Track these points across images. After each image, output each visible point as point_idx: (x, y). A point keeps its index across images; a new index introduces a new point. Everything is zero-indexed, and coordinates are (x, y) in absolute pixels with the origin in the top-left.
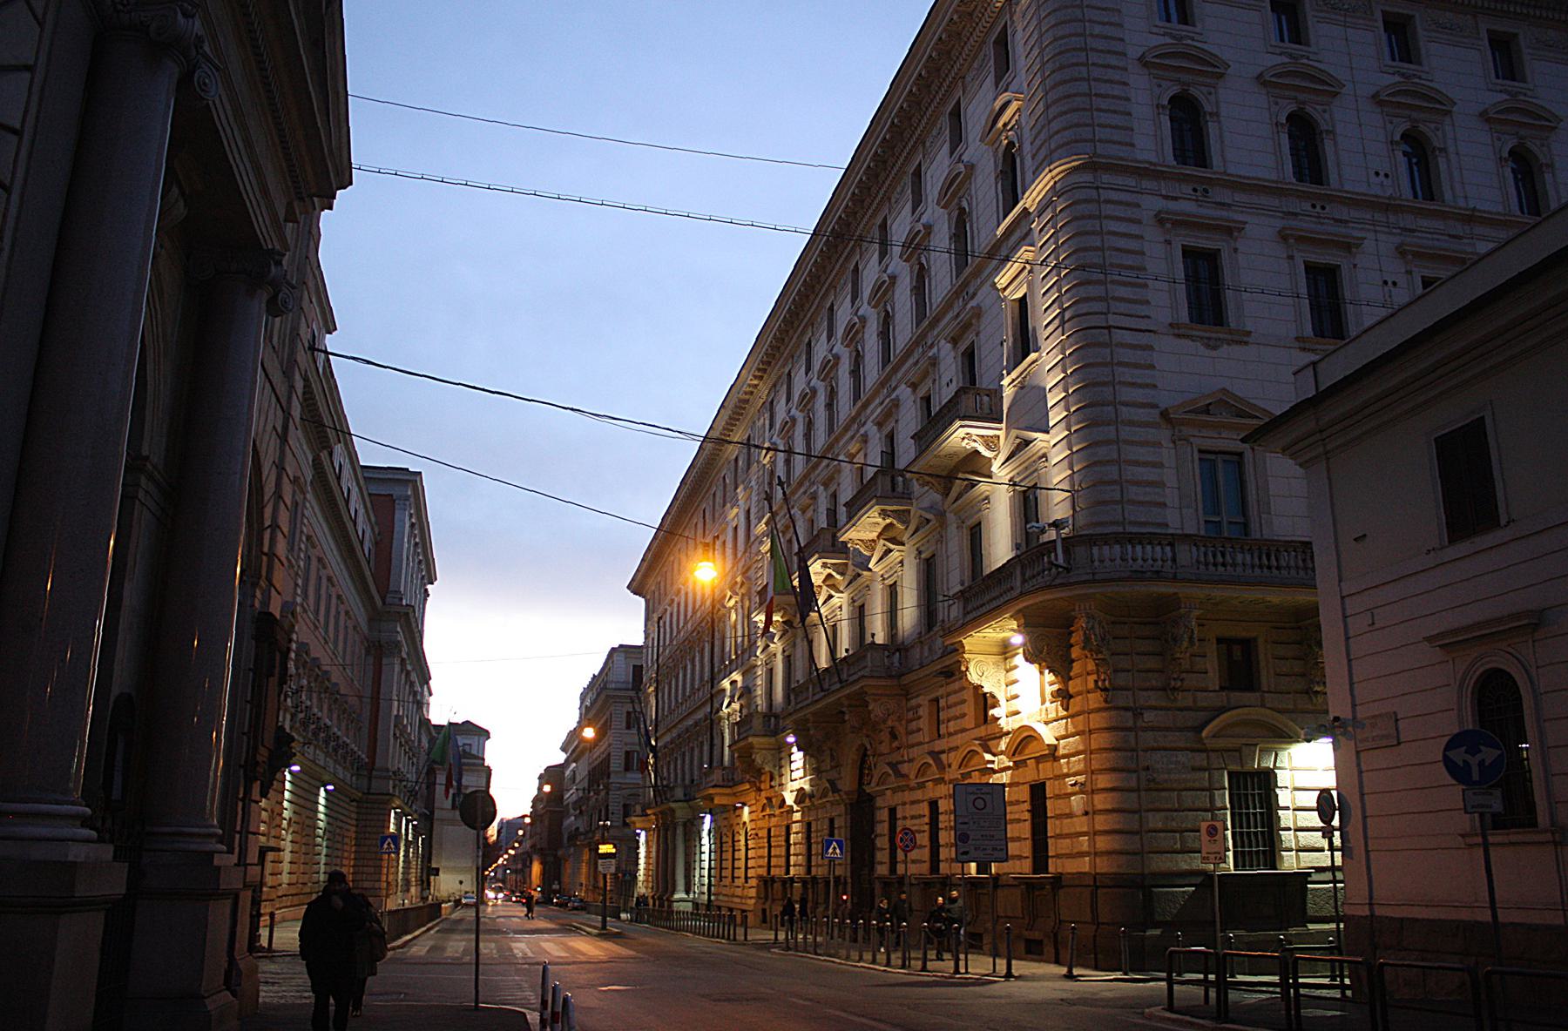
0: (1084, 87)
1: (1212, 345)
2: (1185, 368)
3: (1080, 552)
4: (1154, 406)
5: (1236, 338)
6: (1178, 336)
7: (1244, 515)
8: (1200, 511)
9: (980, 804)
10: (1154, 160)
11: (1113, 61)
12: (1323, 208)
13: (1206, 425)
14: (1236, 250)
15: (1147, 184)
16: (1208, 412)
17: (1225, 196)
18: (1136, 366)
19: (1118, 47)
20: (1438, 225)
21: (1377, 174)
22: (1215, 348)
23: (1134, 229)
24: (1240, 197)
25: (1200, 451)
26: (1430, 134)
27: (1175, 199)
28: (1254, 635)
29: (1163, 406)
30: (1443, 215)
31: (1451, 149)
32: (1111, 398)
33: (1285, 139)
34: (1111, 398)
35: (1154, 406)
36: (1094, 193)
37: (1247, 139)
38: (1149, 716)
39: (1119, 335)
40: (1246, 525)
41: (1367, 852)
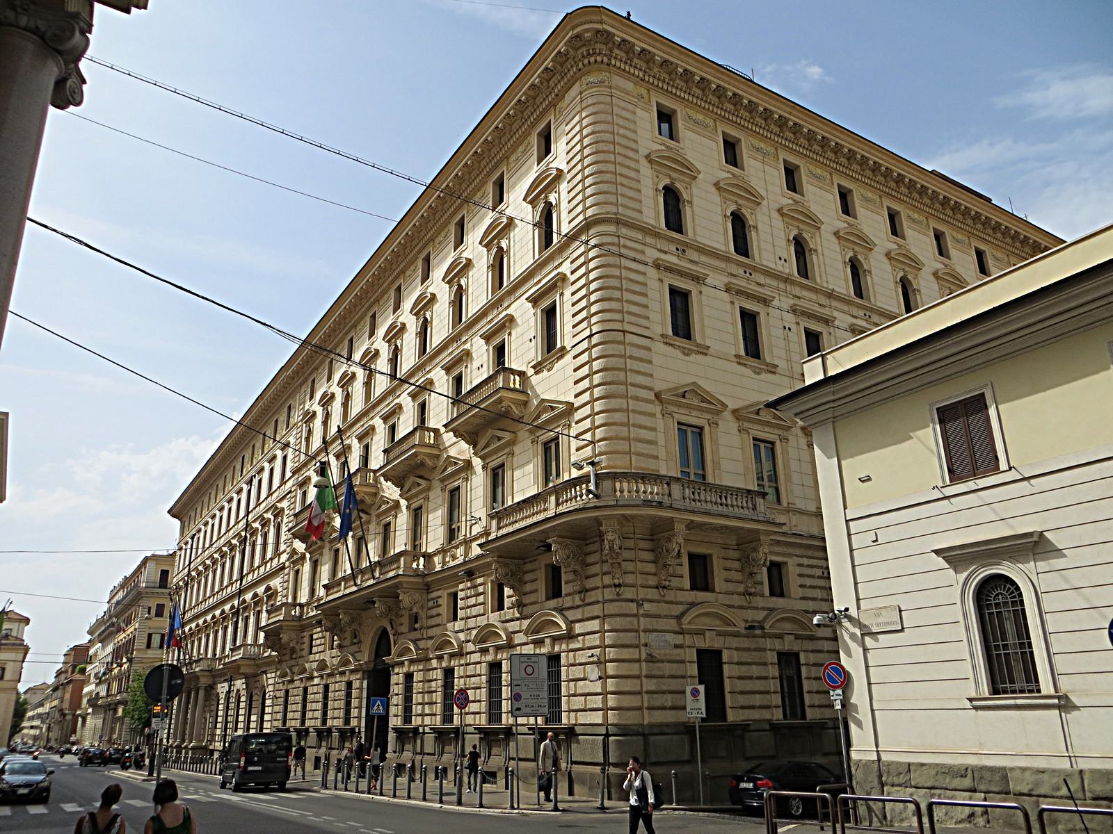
0: (611, 167)
1: (686, 353)
2: (671, 367)
3: (607, 484)
4: (651, 389)
5: (700, 350)
6: (666, 343)
7: (703, 469)
8: (679, 466)
9: (529, 670)
10: (654, 224)
11: (631, 154)
12: (751, 274)
13: (680, 405)
14: (701, 292)
15: (649, 240)
16: (684, 396)
17: (694, 256)
18: (641, 360)
19: (633, 145)
20: (813, 296)
21: (780, 259)
22: (687, 355)
23: (641, 268)
24: (703, 259)
25: (679, 423)
26: (808, 239)
27: (665, 252)
28: (710, 552)
29: (657, 389)
30: (815, 291)
31: (820, 251)
32: (624, 380)
33: (730, 225)
34: (624, 380)
35: (651, 389)
36: (615, 240)
37: (708, 222)
38: (647, 606)
39: (629, 338)
40: (704, 477)
41: (873, 711)
